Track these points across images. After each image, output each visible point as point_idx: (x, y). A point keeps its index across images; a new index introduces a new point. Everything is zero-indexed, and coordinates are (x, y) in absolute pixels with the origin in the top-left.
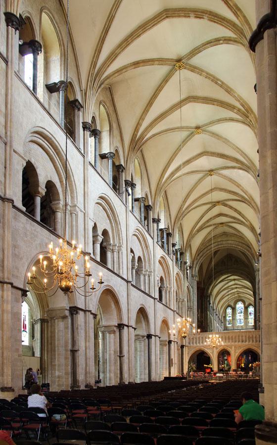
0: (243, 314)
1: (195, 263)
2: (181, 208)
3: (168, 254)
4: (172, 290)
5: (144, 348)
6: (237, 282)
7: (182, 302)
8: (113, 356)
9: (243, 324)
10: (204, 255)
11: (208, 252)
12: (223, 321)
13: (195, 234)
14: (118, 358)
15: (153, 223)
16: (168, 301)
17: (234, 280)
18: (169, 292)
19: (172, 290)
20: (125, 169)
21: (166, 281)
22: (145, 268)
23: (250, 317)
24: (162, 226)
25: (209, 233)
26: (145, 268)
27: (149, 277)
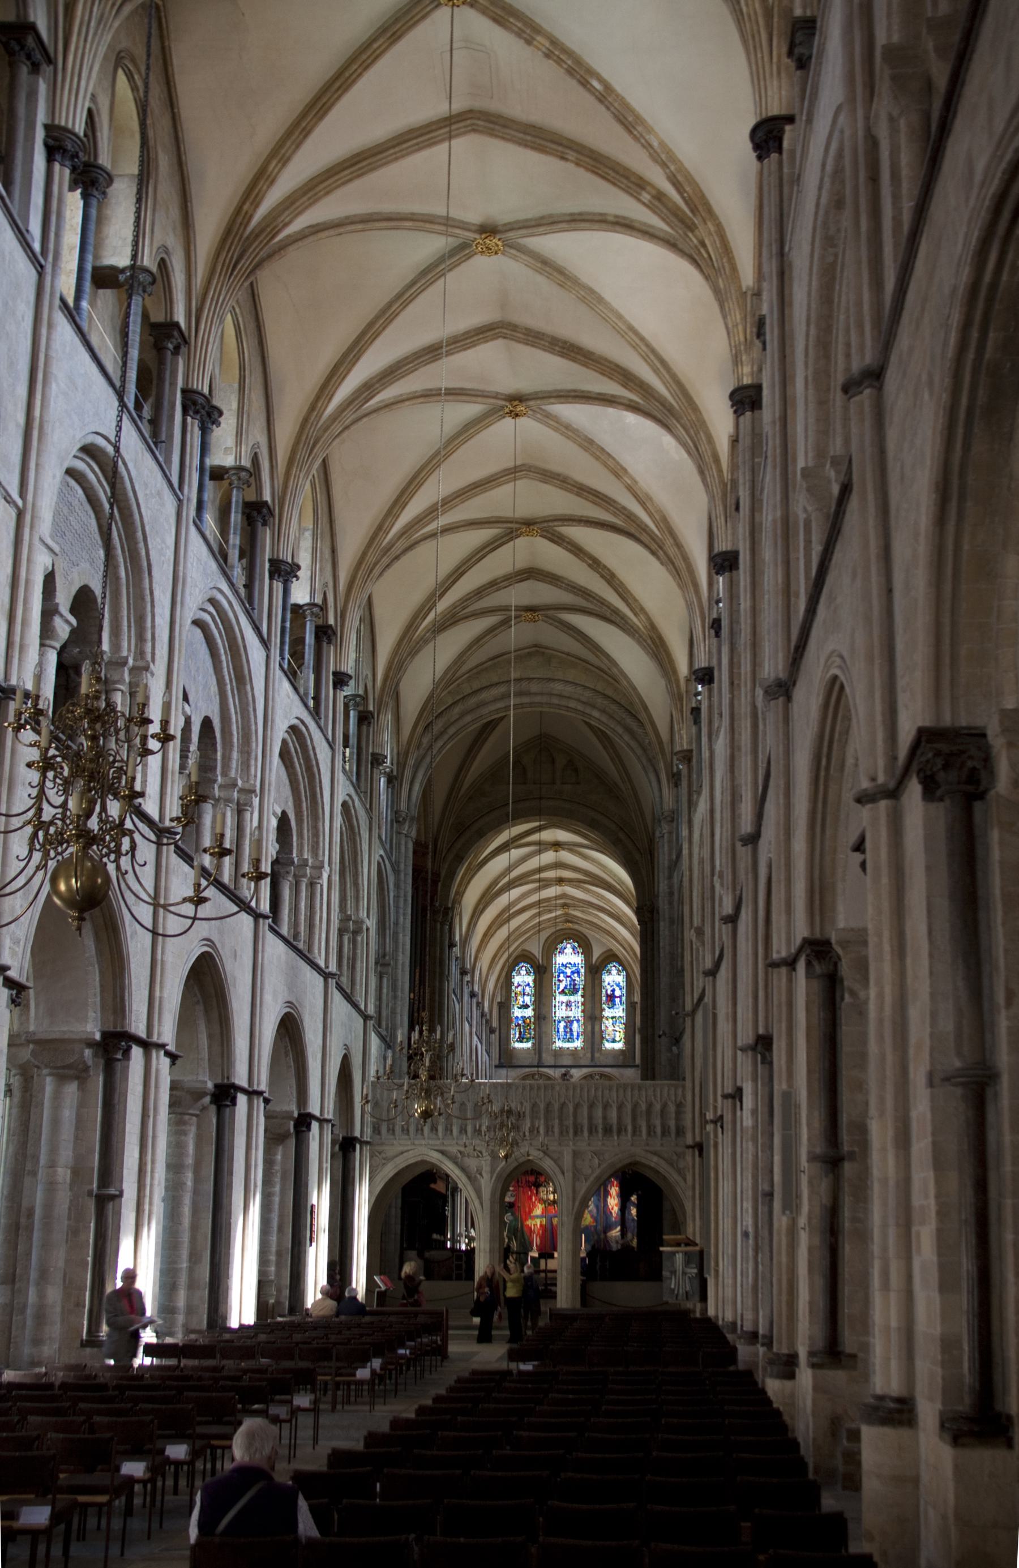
0: (578, 998)
1: (411, 762)
2: (380, 529)
3: (316, 713)
4: (325, 876)
5: (198, 1147)
6: (566, 856)
7: (356, 932)
8: (63, 1198)
9: (578, 1044)
10: (452, 731)
11: (468, 718)
12: (495, 1024)
13: (424, 641)
14: (91, 1205)
15: (271, 578)
16: (302, 928)
17: (557, 845)
18: (312, 885)
19: (325, 876)
20: (186, 342)
21: (300, 835)
22: (225, 774)
23: (608, 1013)
24: (300, 594)
25: (477, 642)
26: (225, 774)
27: (240, 812)
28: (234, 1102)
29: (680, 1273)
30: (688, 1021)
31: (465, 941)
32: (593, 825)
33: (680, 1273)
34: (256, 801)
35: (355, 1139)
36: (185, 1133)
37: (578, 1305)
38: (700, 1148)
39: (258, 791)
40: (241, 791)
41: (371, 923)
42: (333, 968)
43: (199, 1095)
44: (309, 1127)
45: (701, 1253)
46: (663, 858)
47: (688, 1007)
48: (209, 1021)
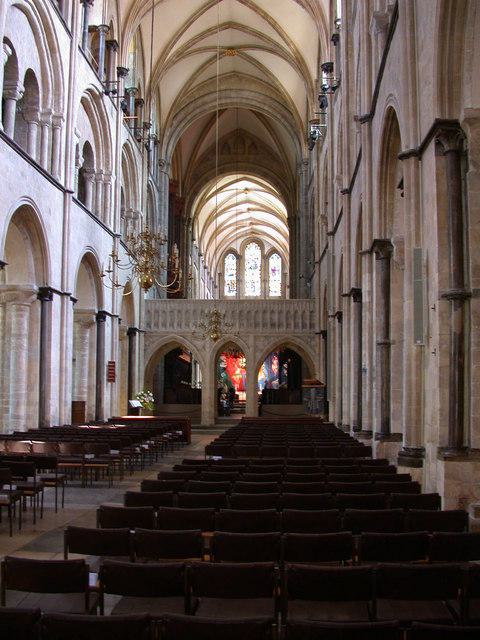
1: (167, 133)
4: (113, 181)
7: (135, 218)
10: (189, 118)
18: (105, 185)
19: (113, 181)
25: (202, 68)
27: (54, 130)
28: (51, 299)
29: (313, 398)
30: (317, 268)
31: (201, 239)
32: (265, 176)
33: (313, 398)
34: (64, 124)
35: (136, 329)
36: (22, 316)
37: (256, 415)
38: (324, 334)
39: (65, 118)
40: (54, 117)
41: (143, 214)
42: (118, 232)
43: (29, 293)
44: (104, 318)
45: (325, 388)
46: (303, 184)
47: (317, 259)
48: (34, 250)
